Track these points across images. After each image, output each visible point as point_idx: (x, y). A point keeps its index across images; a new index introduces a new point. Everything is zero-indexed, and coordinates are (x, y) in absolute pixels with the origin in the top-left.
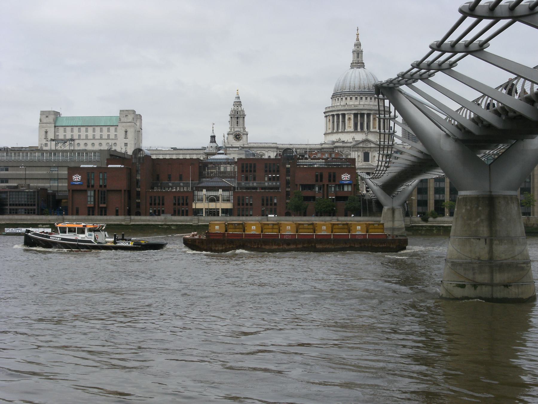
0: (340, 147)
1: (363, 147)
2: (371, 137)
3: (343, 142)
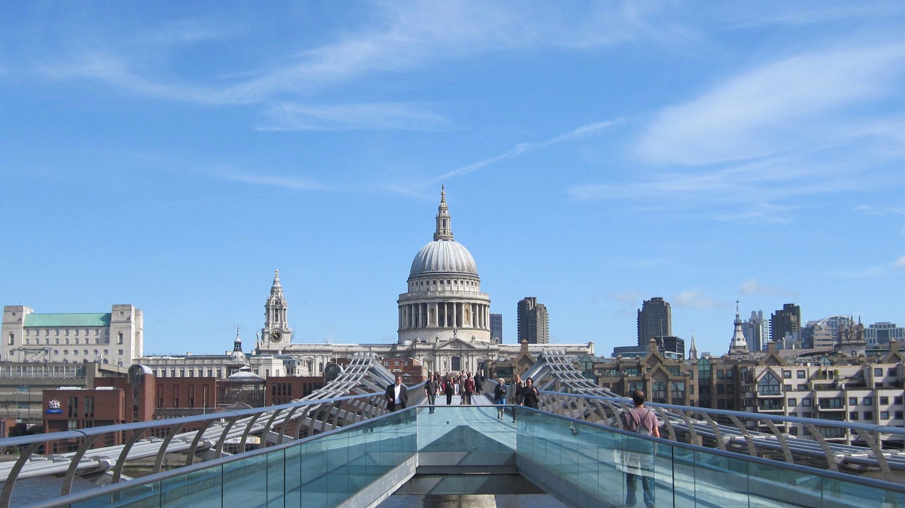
0: (420, 350)
2: (464, 336)
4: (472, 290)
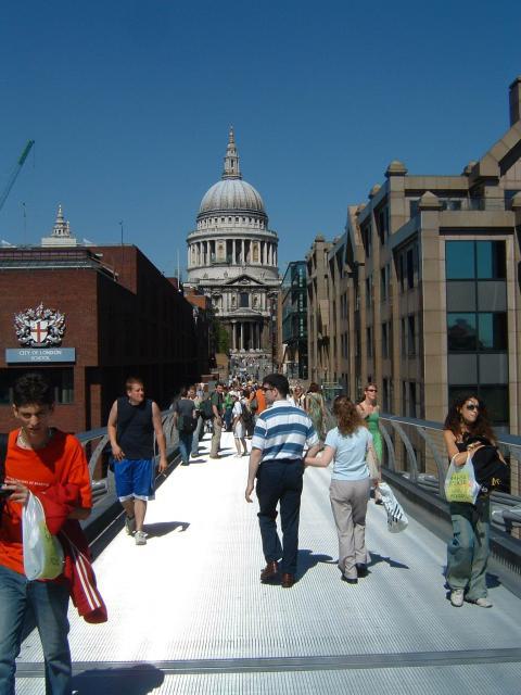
3: (213, 279)
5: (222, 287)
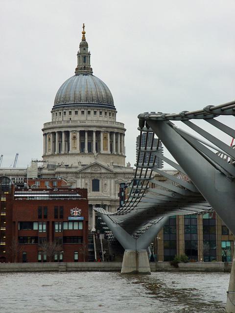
0: (63, 173)
1: (92, 173)
4: (110, 120)
5: (76, 173)
